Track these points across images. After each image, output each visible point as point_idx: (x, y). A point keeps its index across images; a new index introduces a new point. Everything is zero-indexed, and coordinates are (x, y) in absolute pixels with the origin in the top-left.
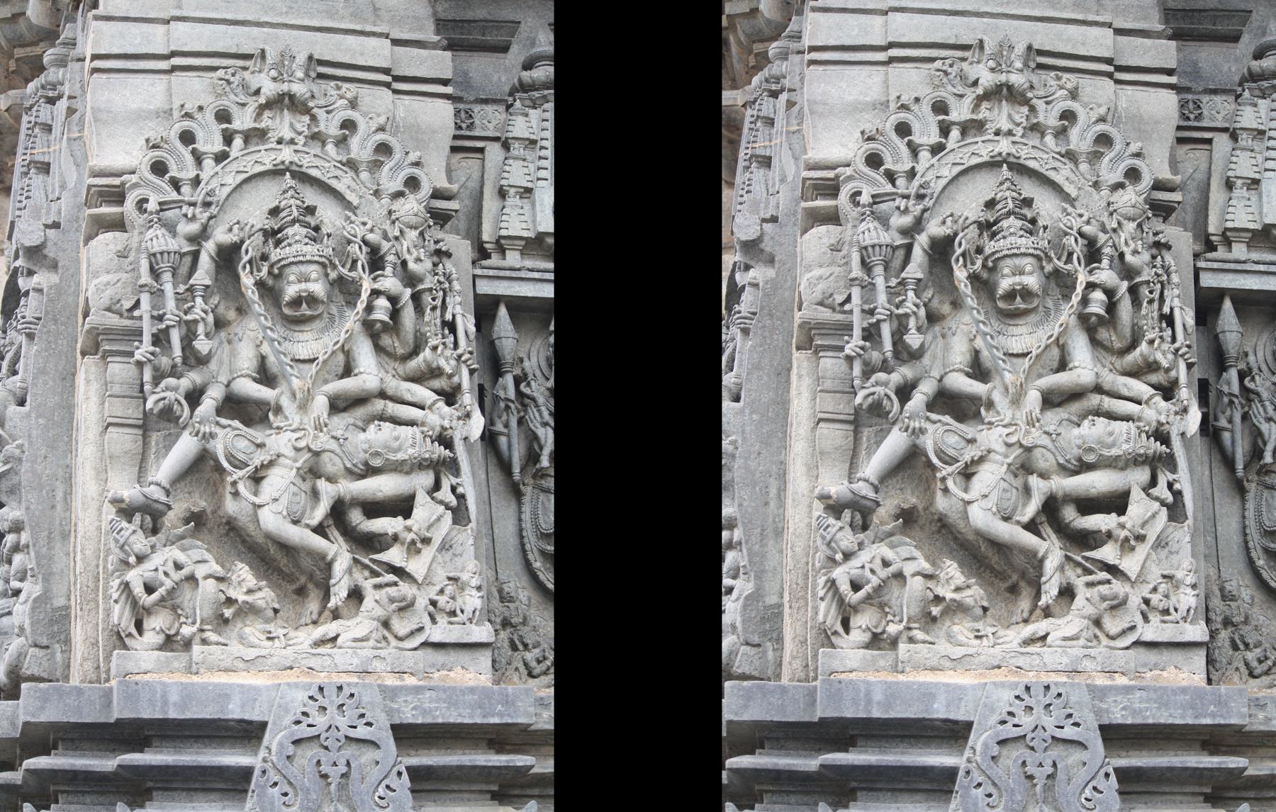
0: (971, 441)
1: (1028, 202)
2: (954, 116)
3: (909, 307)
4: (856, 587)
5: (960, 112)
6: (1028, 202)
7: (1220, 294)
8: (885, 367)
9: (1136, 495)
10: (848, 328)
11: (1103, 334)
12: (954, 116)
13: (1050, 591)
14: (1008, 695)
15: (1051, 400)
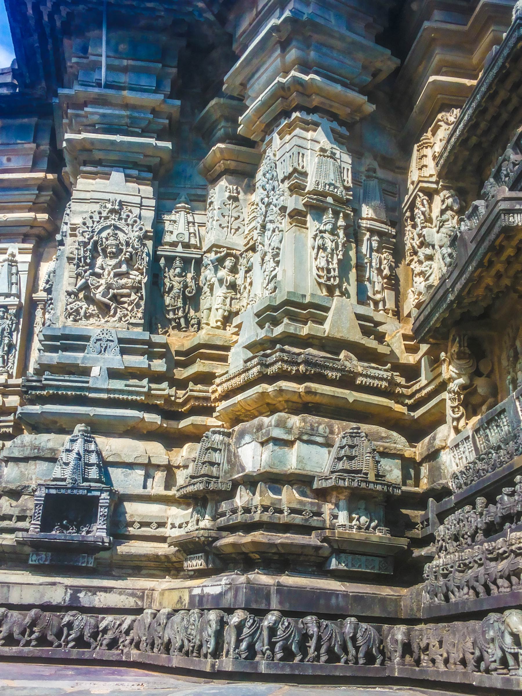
0: (99, 282)
1: (116, 234)
2: (103, 215)
3: (88, 254)
4: (71, 309)
5: (104, 214)
6: (116, 234)
7: (162, 256)
8: (83, 267)
9: (133, 294)
10: (75, 259)
11: (130, 262)
12: (103, 215)
13: (112, 312)
14: (99, 331)
15: (116, 275)
